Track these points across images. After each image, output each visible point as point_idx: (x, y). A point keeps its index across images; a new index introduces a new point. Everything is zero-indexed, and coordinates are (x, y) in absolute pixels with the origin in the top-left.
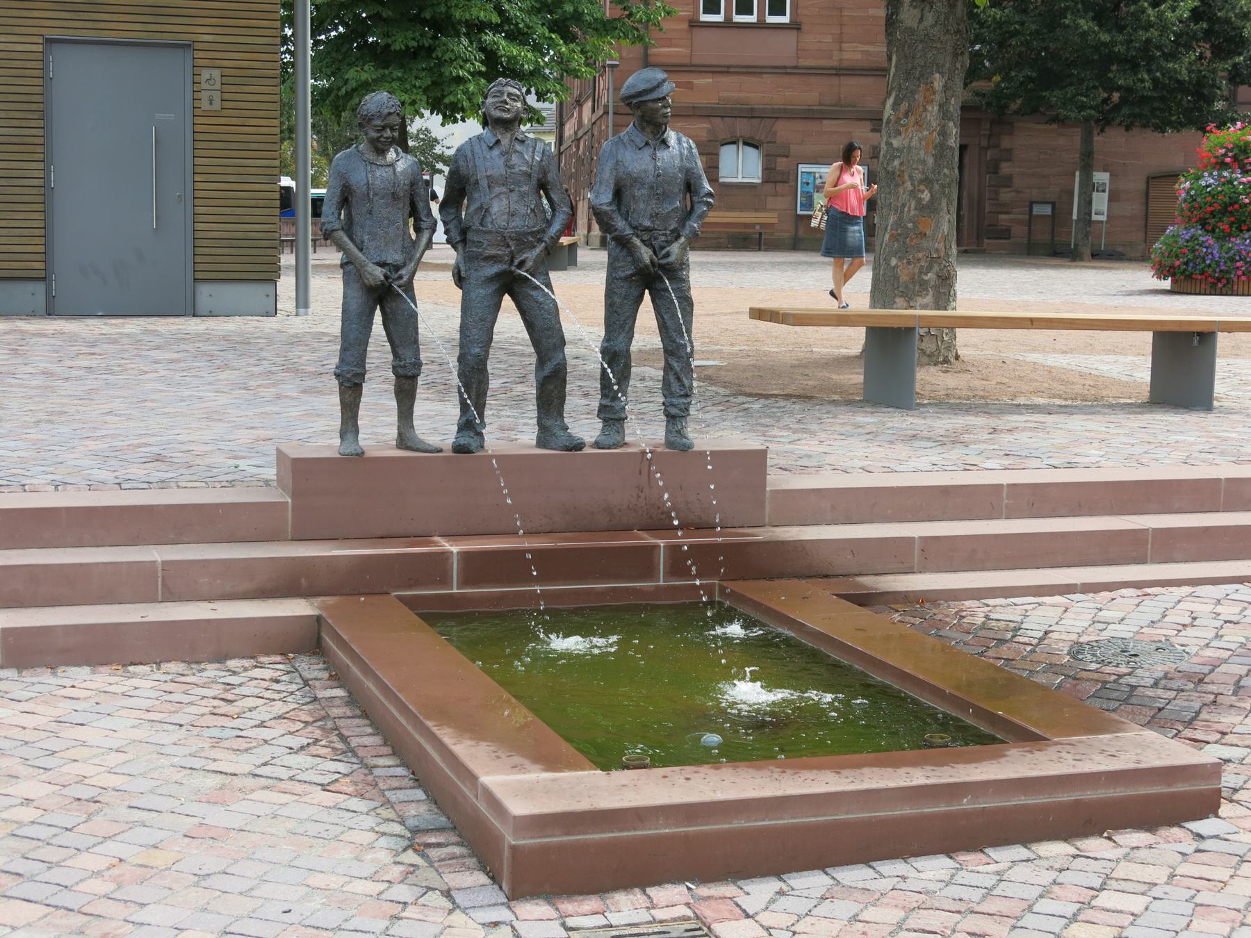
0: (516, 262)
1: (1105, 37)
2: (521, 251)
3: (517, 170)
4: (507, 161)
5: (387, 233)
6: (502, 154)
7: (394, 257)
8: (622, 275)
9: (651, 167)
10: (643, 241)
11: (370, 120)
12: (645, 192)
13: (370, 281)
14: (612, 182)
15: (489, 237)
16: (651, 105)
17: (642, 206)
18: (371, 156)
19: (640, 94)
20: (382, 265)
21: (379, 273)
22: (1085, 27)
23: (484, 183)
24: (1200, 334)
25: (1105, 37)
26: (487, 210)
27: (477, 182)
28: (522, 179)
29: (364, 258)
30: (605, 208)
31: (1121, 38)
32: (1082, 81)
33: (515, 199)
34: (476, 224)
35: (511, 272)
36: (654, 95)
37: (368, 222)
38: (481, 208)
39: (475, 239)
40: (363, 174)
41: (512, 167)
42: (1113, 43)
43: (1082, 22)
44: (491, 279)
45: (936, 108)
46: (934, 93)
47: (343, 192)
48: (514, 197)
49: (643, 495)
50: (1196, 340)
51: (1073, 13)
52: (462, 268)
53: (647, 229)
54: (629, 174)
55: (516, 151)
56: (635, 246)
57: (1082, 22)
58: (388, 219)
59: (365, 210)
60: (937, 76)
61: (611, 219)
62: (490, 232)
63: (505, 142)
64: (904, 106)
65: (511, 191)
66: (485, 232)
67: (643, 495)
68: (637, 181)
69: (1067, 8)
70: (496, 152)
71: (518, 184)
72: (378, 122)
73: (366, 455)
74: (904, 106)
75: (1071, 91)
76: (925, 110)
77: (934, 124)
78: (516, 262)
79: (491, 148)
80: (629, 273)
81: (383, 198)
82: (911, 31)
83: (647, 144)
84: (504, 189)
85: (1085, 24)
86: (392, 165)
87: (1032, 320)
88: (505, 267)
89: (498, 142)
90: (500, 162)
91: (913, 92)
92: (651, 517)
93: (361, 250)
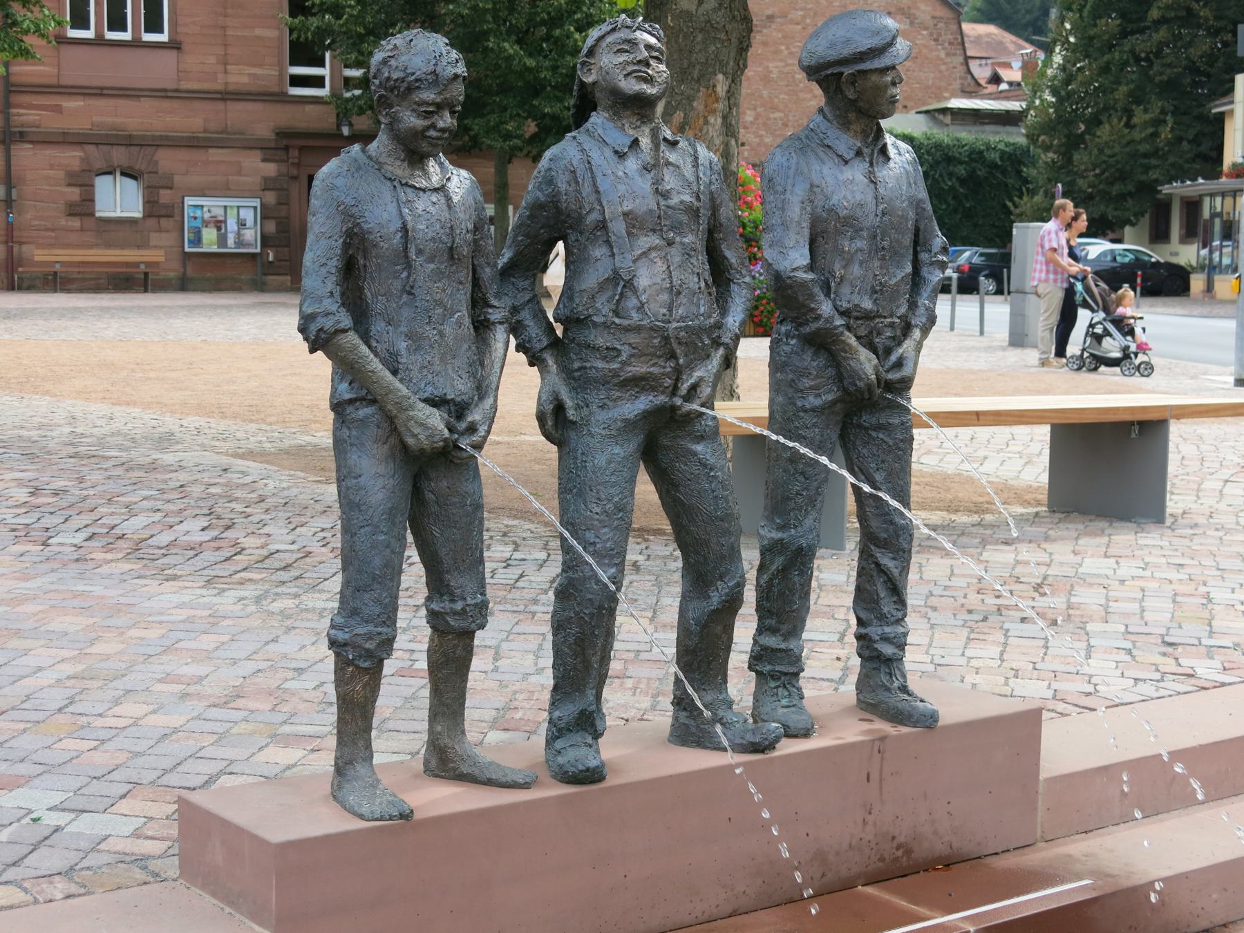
0: (684, 388)
1: (530, 62)
2: (691, 367)
3: (674, 201)
4: (657, 182)
5: (441, 334)
6: (646, 168)
7: (458, 386)
8: (817, 402)
9: (870, 197)
10: (858, 338)
11: (410, 89)
12: (860, 244)
13: (418, 439)
14: (806, 224)
15: (633, 338)
16: (874, 78)
17: (856, 270)
18: (399, 169)
19: (862, 57)
20: (434, 402)
21: (436, 420)
22: (511, 51)
23: (618, 227)
24: (1141, 424)
25: (530, 62)
26: (629, 285)
27: (602, 225)
28: (685, 218)
29: (404, 391)
30: (803, 275)
31: (547, 63)
32: (505, 109)
33: (677, 259)
34: (603, 309)
35: (674, 408)
36: (884, 61)
37: (406, 313)
38: (615, 278)
39: (600, 342)
40: (392, 208)
41: (665, 195)
42: (538, 69)
43: (506, 45)
44: (629, 426)
45: (720, 120)
46: (717, 100)
47: (346, 246)
48: (676, 255)
49: (870, 819)
50: (1137, 428)
51: (495, 36)
52: (569, 403)
53: (868, 316)
54: (831, 210)
55: (668, 164)
56: (848, 349)
57: (506, 45)
58: (440, 303)
59: (397, 285)
60: (720, 77)
61: (812, 296)
62: (638, 329)
63: (645, 142)
64: (678, 116)
65: (670, 243)
66: (627, 329)
67: (870, 819)
68: (849, 223)
69: (491, 30)
70: (632, 164)
71: (677, 227)
72: (429, 95)
73: (418, 816)
74: (678, 116)
75: (493, 119)
76: (706, 122)
77: (717, 142)
78: (684, 388)
79: (621, 156)
80: (830, 397)
81: (431, 259)
82: (687, 15)
83: (859, 153)
84: (655, 240)
85: (510, 48)
86: (441, 189)
87: (978, 414)
88: (662, 399)
89: (635, 143)
90: (644, 184)
91: (691, 99)
92: (882, 859)
93: (395, 372)
